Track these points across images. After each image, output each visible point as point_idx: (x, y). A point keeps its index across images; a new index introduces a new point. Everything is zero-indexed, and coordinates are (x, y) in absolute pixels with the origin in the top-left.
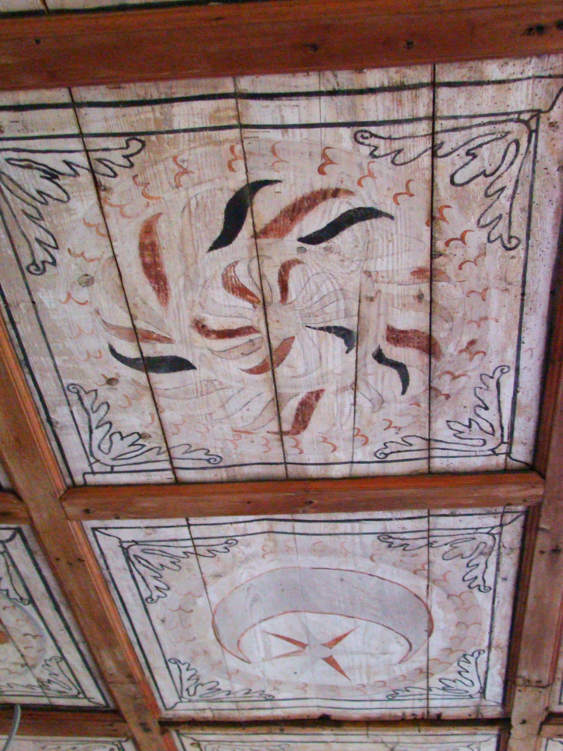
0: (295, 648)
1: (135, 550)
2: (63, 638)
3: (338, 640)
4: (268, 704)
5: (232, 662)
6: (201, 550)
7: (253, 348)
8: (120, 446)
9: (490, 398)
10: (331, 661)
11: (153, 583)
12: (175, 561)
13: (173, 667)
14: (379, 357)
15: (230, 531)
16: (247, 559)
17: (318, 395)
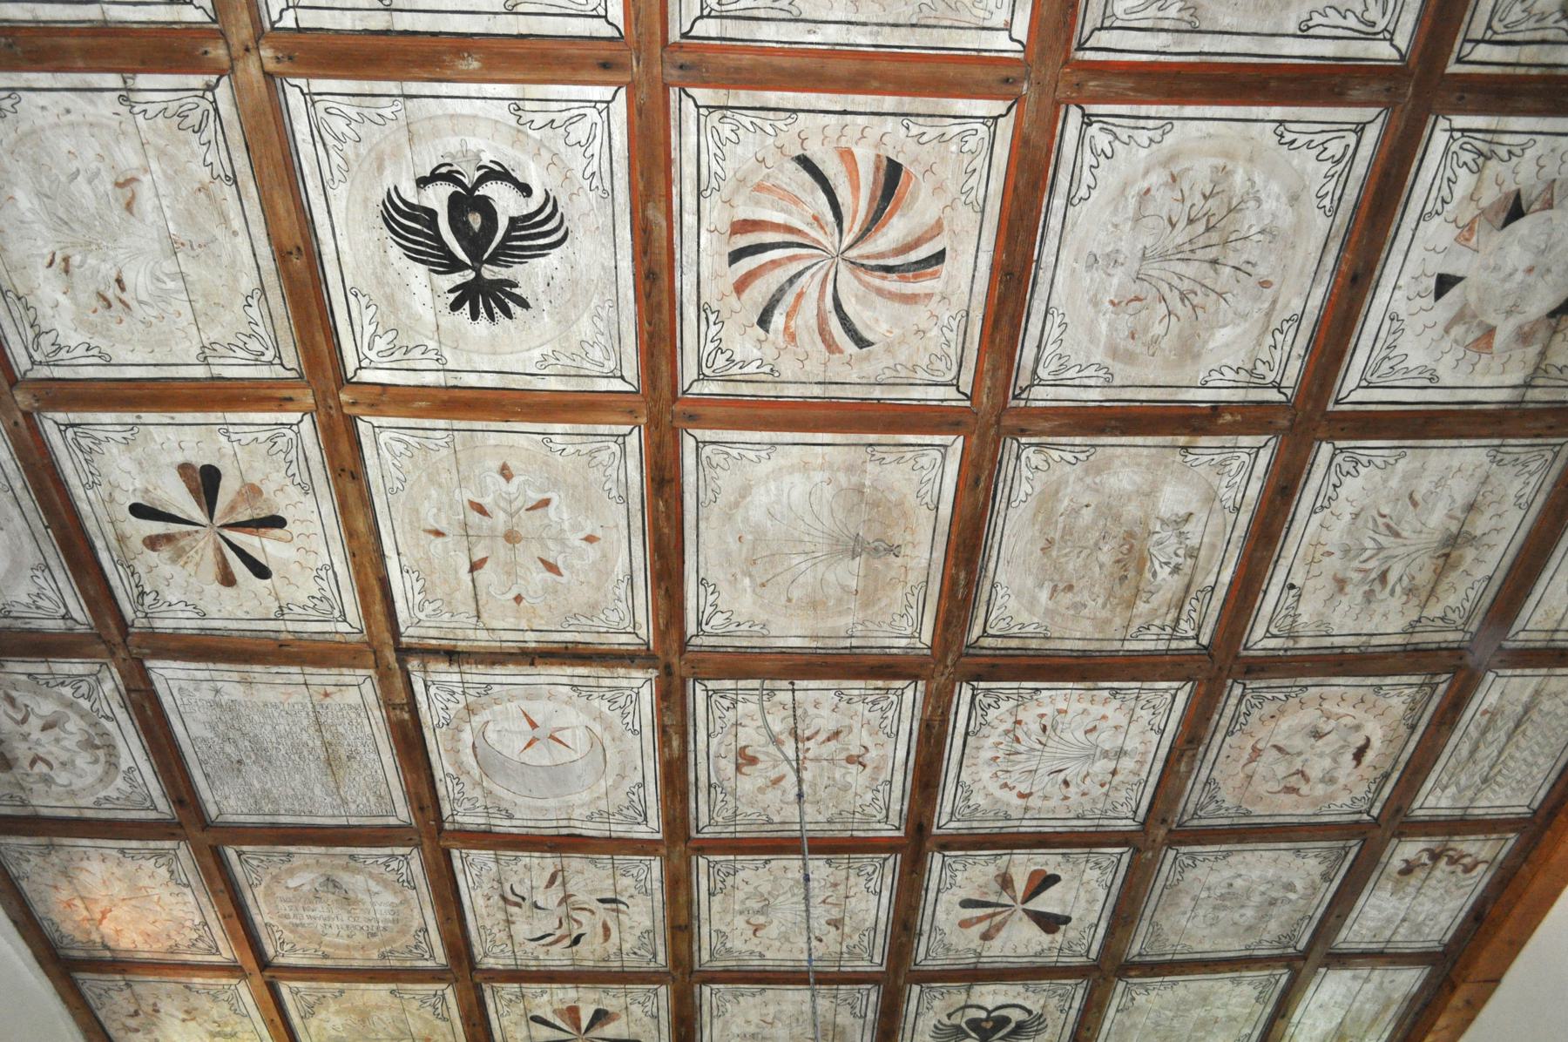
0: (557, 735)
1: (640, 819)
2: (702, 745)
3: (529, 744)
4: (576, 681)
5: (597, 728)
6: (606, 815)
7: (573, 903)
8: (635, 872)
9: (476, 879)
10: (533, 725)
11: (635, 798)
12: (620, 812)
13: (637, 727)
14: (524, 899)
15: (590, 825)
16: (583, 805)
17: (547, 887)
